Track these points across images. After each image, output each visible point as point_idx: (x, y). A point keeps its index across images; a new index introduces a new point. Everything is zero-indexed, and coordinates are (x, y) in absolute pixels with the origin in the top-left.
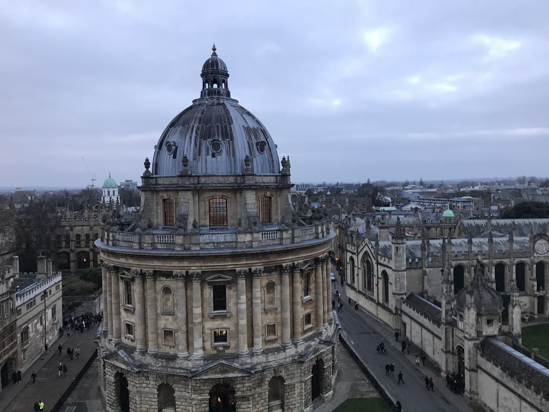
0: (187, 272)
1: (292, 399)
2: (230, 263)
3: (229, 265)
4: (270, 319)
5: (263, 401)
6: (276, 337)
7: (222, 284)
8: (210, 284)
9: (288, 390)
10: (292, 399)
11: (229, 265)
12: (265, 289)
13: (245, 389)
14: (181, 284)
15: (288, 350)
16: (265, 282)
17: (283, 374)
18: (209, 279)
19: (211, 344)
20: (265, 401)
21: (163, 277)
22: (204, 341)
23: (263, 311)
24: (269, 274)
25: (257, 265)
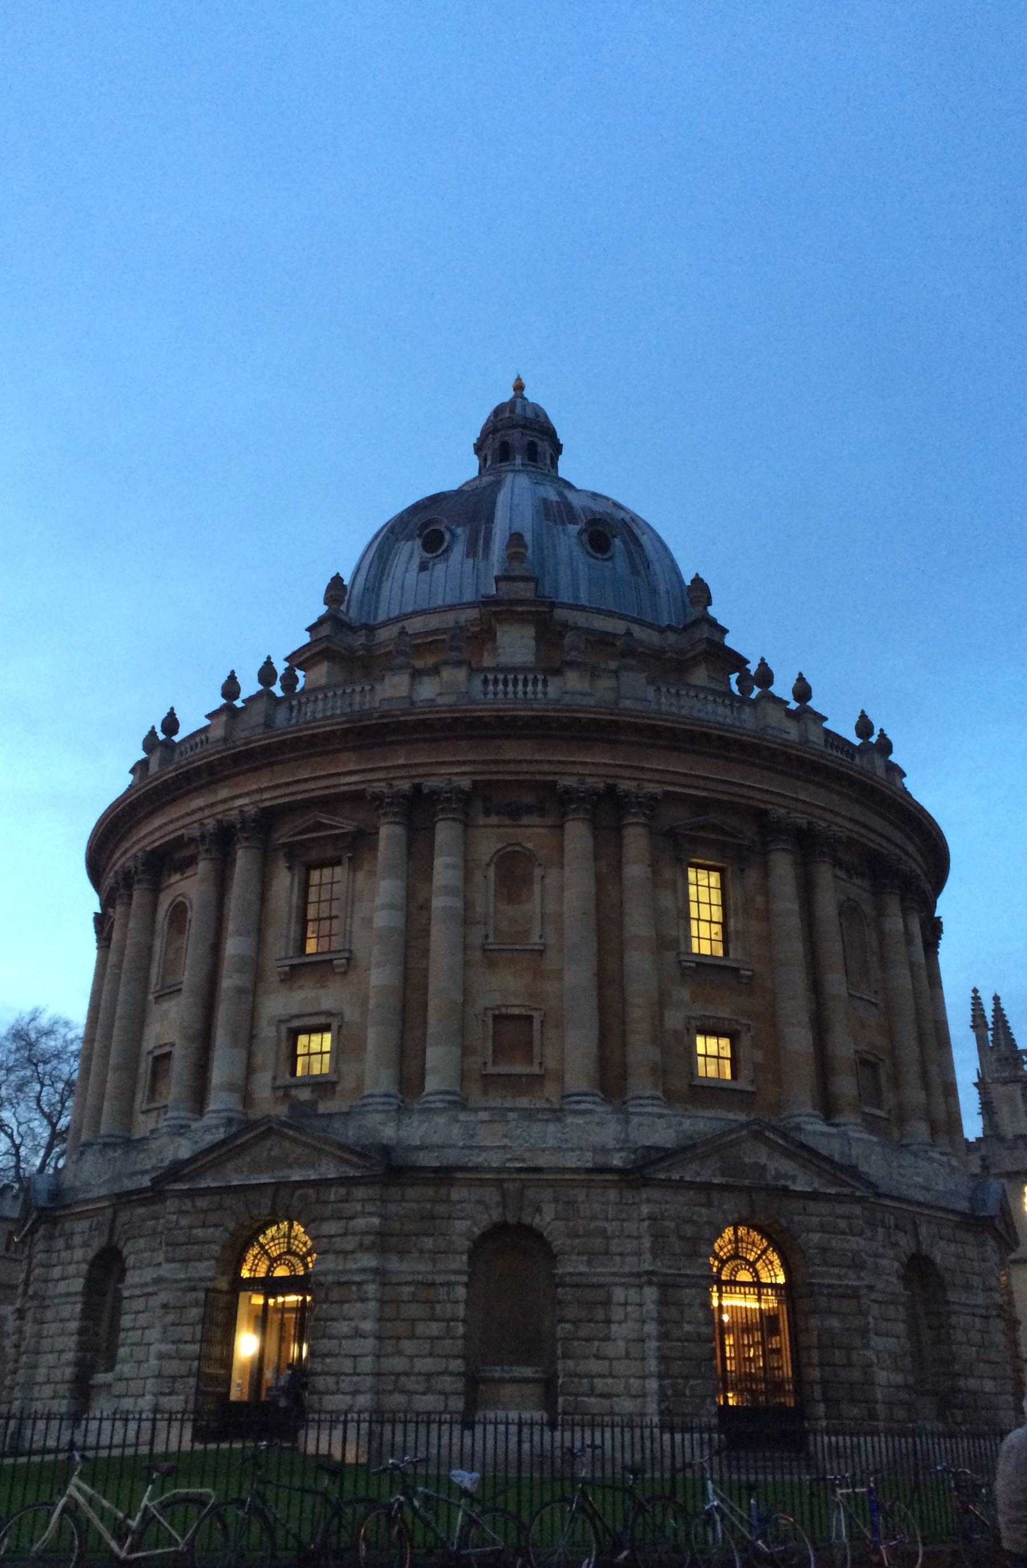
0: (220, 822)
1: (596, 1366)
2: (351, 767)
3: (347, 772)
4: (504, 988)
5: (435, 1328)
6: (536, 1070)
7: (330, 853)
8: (293, 853)
9: (574, 1312)
10: (596, 1366)
11: (347, 772)
12: (491, 872)
13: (350, 1243)
14: (203, 867)
15: (580, 1120)
16: (488, 845)
17: (546, 1219)
18: (283, 835)
19: (274, 1078)
20: (449, 1334)
21: (176, 872)
22: (250, 1070)
23: (477, 955)
24: (508, 822)
25: (451, 769)
